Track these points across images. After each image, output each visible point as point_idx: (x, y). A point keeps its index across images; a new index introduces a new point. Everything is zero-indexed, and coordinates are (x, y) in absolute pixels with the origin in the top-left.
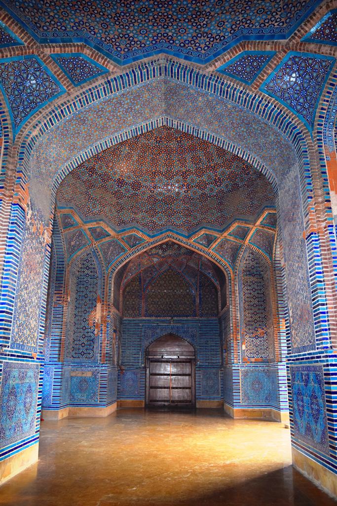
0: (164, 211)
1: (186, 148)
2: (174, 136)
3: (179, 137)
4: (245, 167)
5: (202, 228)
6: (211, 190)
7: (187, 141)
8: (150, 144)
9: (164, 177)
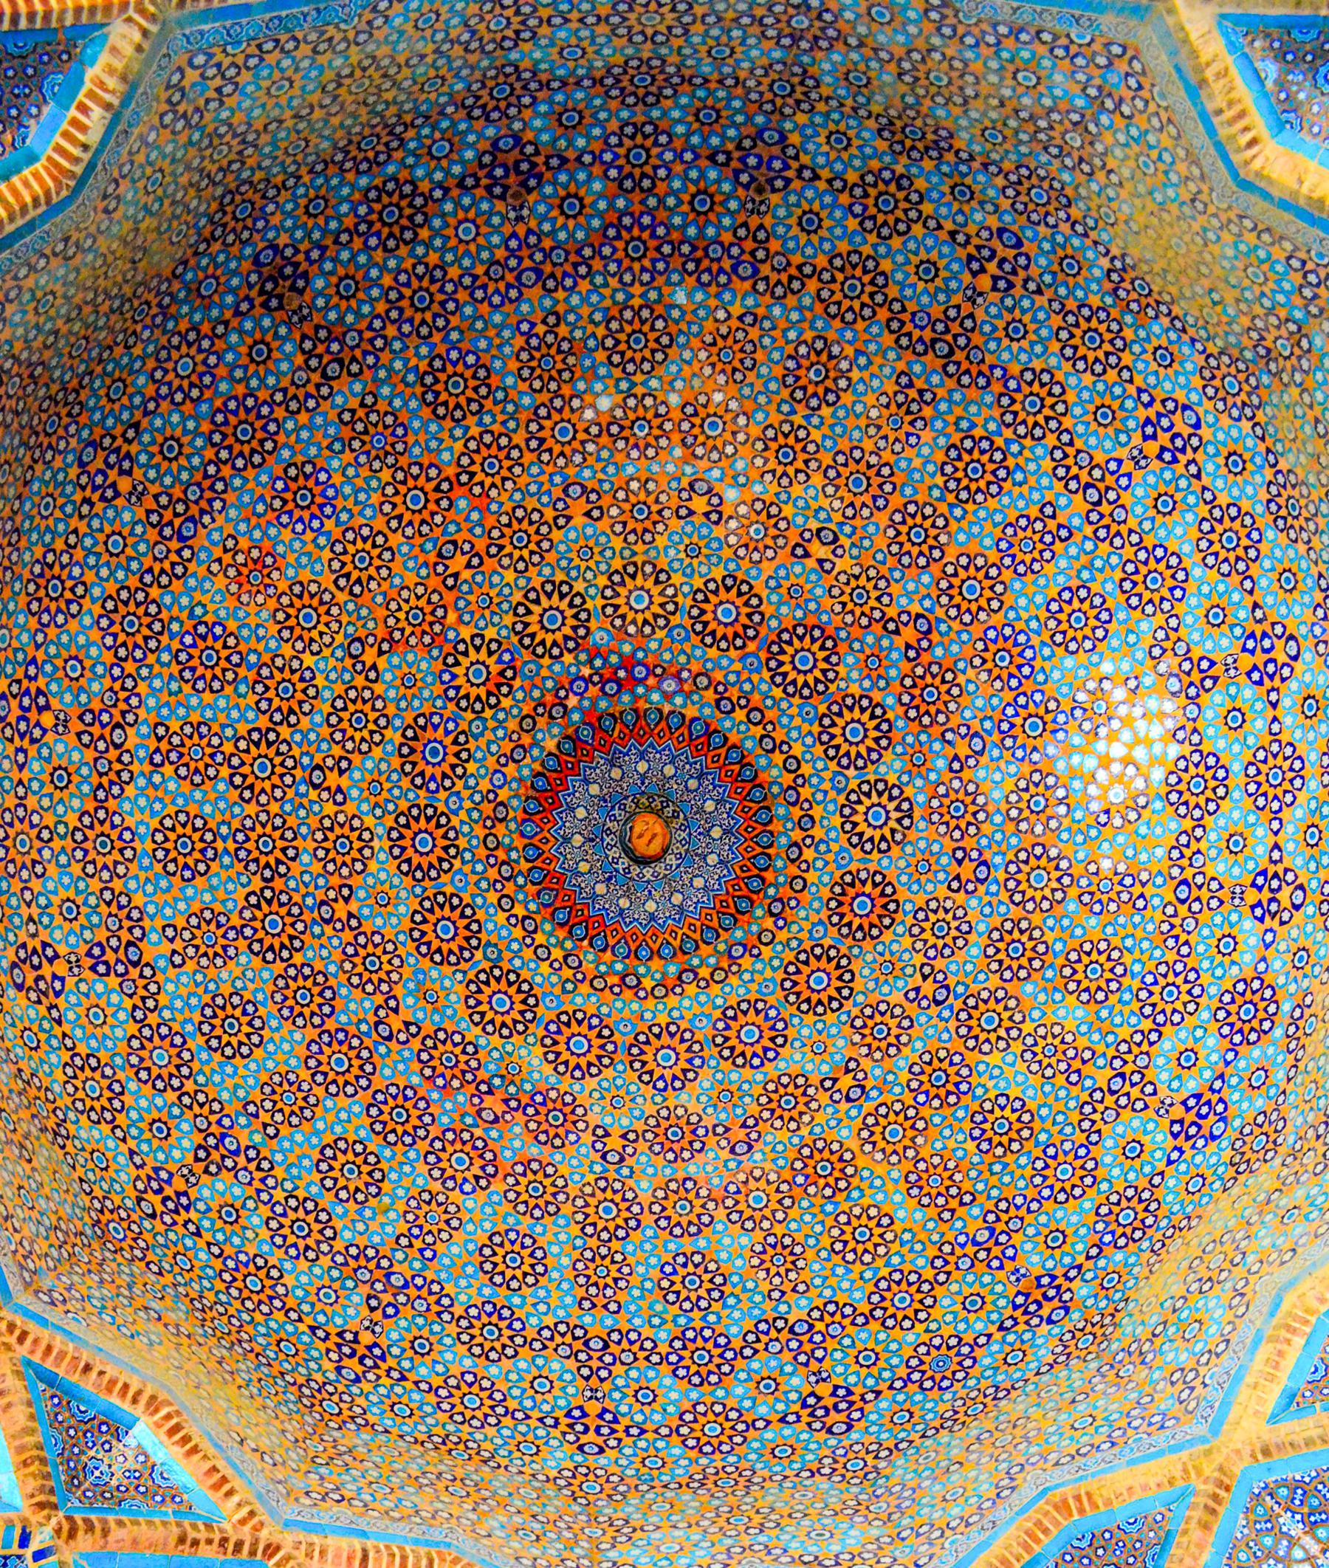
4: (985, 282)
6: (1234, 461)
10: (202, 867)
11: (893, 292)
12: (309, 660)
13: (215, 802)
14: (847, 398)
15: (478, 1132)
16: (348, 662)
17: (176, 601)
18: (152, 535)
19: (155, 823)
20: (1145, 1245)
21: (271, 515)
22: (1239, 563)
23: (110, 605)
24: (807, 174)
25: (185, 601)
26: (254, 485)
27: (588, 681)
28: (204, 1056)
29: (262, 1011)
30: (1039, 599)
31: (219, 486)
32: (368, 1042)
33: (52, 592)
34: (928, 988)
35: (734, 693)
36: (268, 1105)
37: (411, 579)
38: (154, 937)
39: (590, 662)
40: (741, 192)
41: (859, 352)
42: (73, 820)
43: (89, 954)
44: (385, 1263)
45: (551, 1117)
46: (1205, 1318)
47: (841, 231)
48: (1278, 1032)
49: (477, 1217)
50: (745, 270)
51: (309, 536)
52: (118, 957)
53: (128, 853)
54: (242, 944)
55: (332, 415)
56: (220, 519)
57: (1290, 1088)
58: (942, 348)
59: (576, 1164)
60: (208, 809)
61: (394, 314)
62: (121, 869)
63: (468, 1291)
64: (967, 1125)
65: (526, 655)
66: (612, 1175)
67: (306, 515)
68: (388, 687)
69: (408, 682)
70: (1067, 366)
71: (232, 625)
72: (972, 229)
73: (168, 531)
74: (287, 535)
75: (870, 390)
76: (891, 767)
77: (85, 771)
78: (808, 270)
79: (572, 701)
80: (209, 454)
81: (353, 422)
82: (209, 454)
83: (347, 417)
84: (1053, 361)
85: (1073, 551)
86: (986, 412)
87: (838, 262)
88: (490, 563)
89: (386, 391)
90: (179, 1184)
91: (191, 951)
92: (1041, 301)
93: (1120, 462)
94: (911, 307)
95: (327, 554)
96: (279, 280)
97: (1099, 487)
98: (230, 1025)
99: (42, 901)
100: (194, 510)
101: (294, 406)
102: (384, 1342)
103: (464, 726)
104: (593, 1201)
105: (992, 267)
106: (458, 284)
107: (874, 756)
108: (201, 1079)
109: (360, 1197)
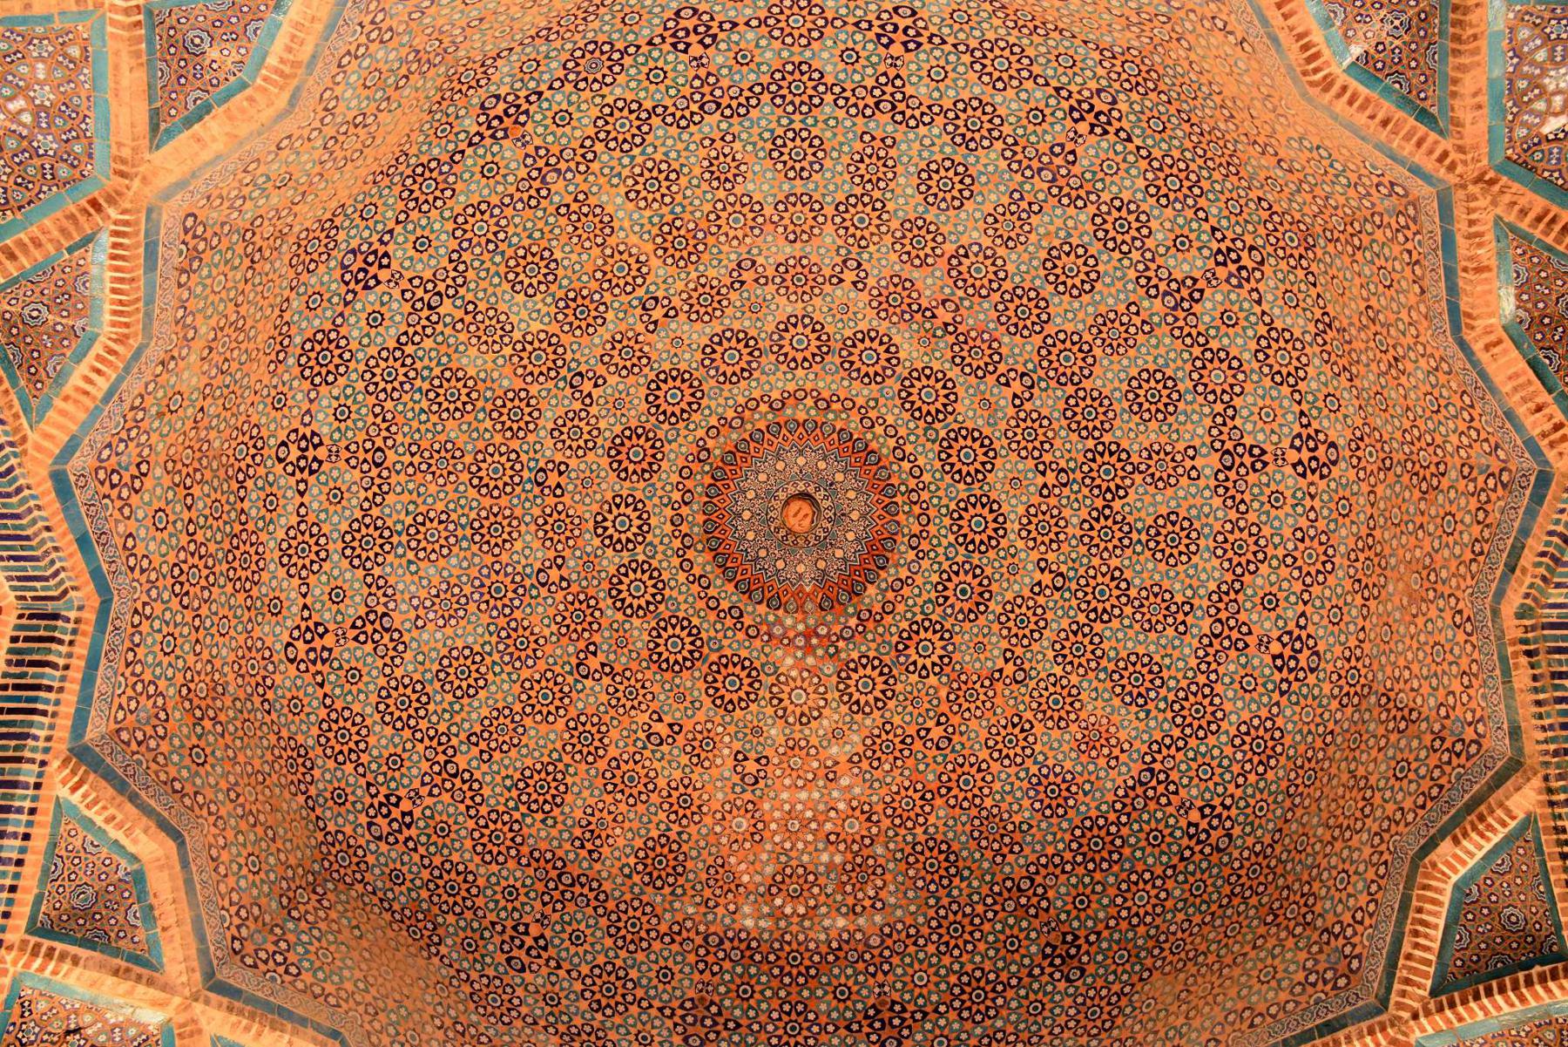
0: (199, 537)
1: (517, 614)
2: (567, 553)
3: (564, 572)
4: (534, 930)
5: (176, 836)
7: (552, 611)
8: (531, 438)
9: (358, 514)
10: (1161, 522)
11: (603, 922)
12: (1058, 670)
13: (1144, 570)
14: (639, 843)
15: (961, 293)
16: (1026, 666)
17: (1159, 724)
18: (1174, 776)
19: (1195, 559)
20: (413, 161)
21: (1080, 780)
22: (336, 719)
23: (1214, 727)
24: (667, 1012)
25: (1152, 724)
26: (1088, 806)
27: (840, 637)
28: (1180, 374)
29: (1126, 405)
30: (493, 688)
31: (1118, 806)
32: (1041, 373)
33: (1261, 743)
34: (587, 386)
35: (729, 622)
36: (1132, 330)
37: (973, 724)
38: (1208, 471)
39: (838, 651)
40: (717, 999)
41: (629, 877)
42: (1264, 569)
43: (1265, 464)
44: (1055, 191)
45: (898, 301)
46: (360, 90)
47: (643, 967)
48: (298, 340)
49: (970, 225)
50: (714, 940)
51: (1050, 763)
52: (1241, 459)
53: (1220, 538)
54: (1135, 459)
55: (1027, 850)
56: (1119, 781)
57: (286, 293)
58: (566, 880)
59: (883, 261)
60: (1150, 566)
61: (977, 921)
62: (1228, 526)
63: (988, 161)
64: (560, 272)
65: (887, 660)
66: (855, 249)
67: (1052, 778)
68: (997, 646)
69: (980, 647)
70: (471, 867)
71: (1117, 702)
72: (545, 970)
73: (1162, 777)
74: (1068, 765)
75: (621, 845)
76: (611, 561)
77: (1248, 605)
78: (667, 939)
79: (853, 622)
80: (1125, 831)
81: (1012, 844)
82: (1125, 831)
83: (1016, 848)
84: (482, 870)
85: (466, 725)
86: (533, 831)
87: (644, 945)
88: (911, 731)
89: (986, 865)
90: (1222, 272)
91: (1178, 458)
92: (492, 917)
93: (430, 794)
94: (590, 910)
95: (1038, 748)
96: (1065, 955)
97: (447, 773)
98: (1155, 396)
99: (1300, 510)
100: (1139, 790)
101: (1057, 860)
102: (1069, 123)
103: (939, 610)
104: (873, 229)
105: (529, 942)
106: (928, 940)
107: (624, 570)
108: (1186, 356)
109: (1067, 248)
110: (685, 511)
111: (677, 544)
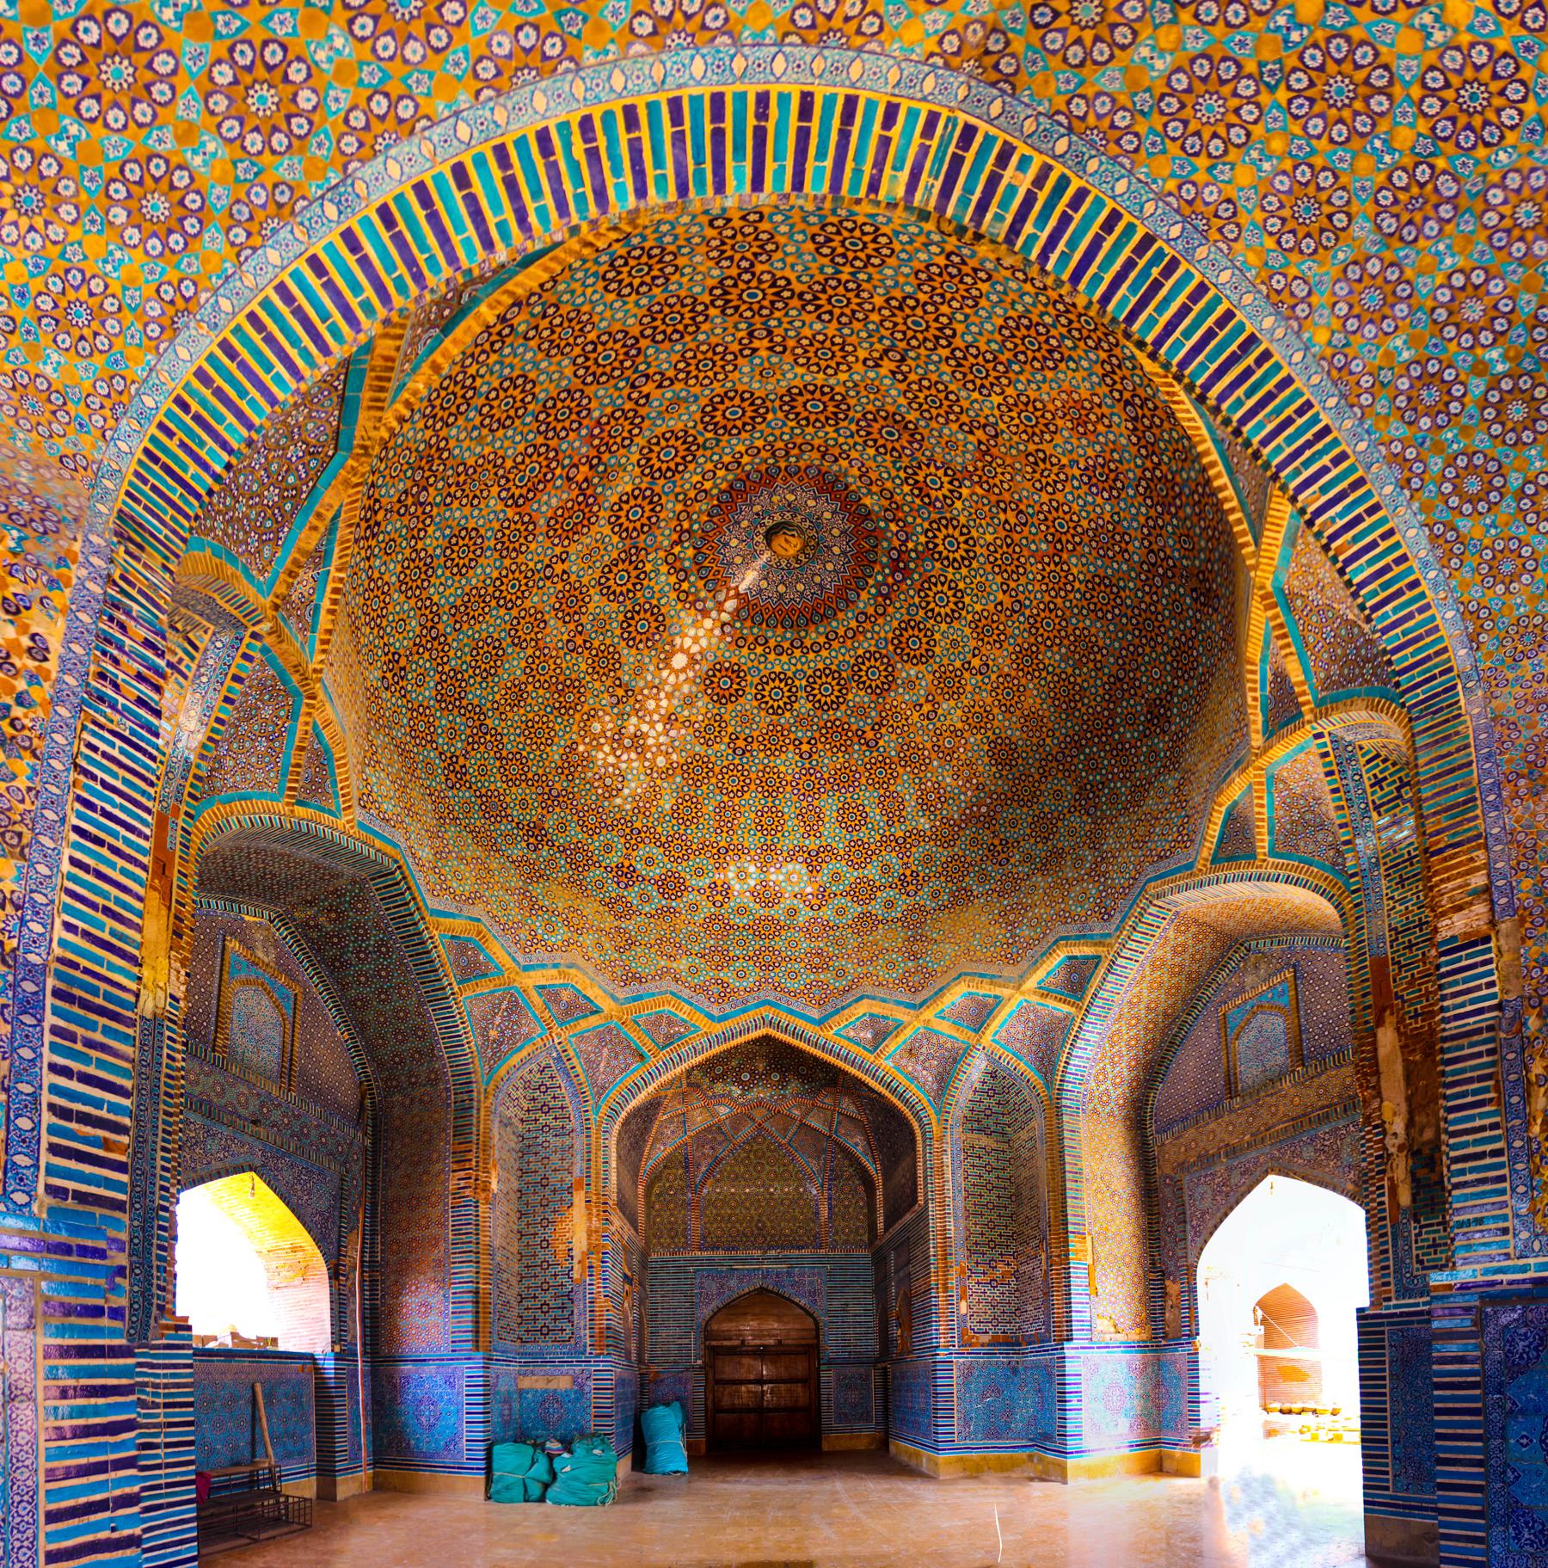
22: (853, 893)
65: (934, 516)
69: (951, 445)
76: (803, 706)
110: (772, 643)
111: (797, 653)
